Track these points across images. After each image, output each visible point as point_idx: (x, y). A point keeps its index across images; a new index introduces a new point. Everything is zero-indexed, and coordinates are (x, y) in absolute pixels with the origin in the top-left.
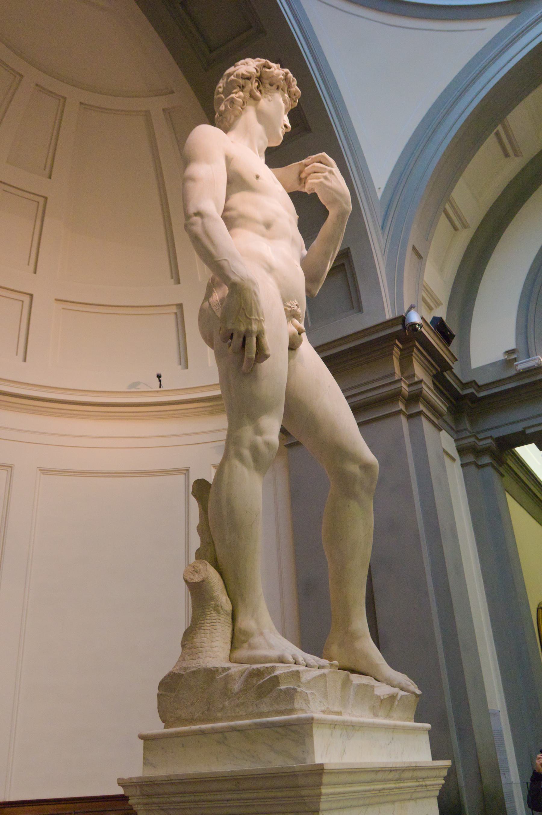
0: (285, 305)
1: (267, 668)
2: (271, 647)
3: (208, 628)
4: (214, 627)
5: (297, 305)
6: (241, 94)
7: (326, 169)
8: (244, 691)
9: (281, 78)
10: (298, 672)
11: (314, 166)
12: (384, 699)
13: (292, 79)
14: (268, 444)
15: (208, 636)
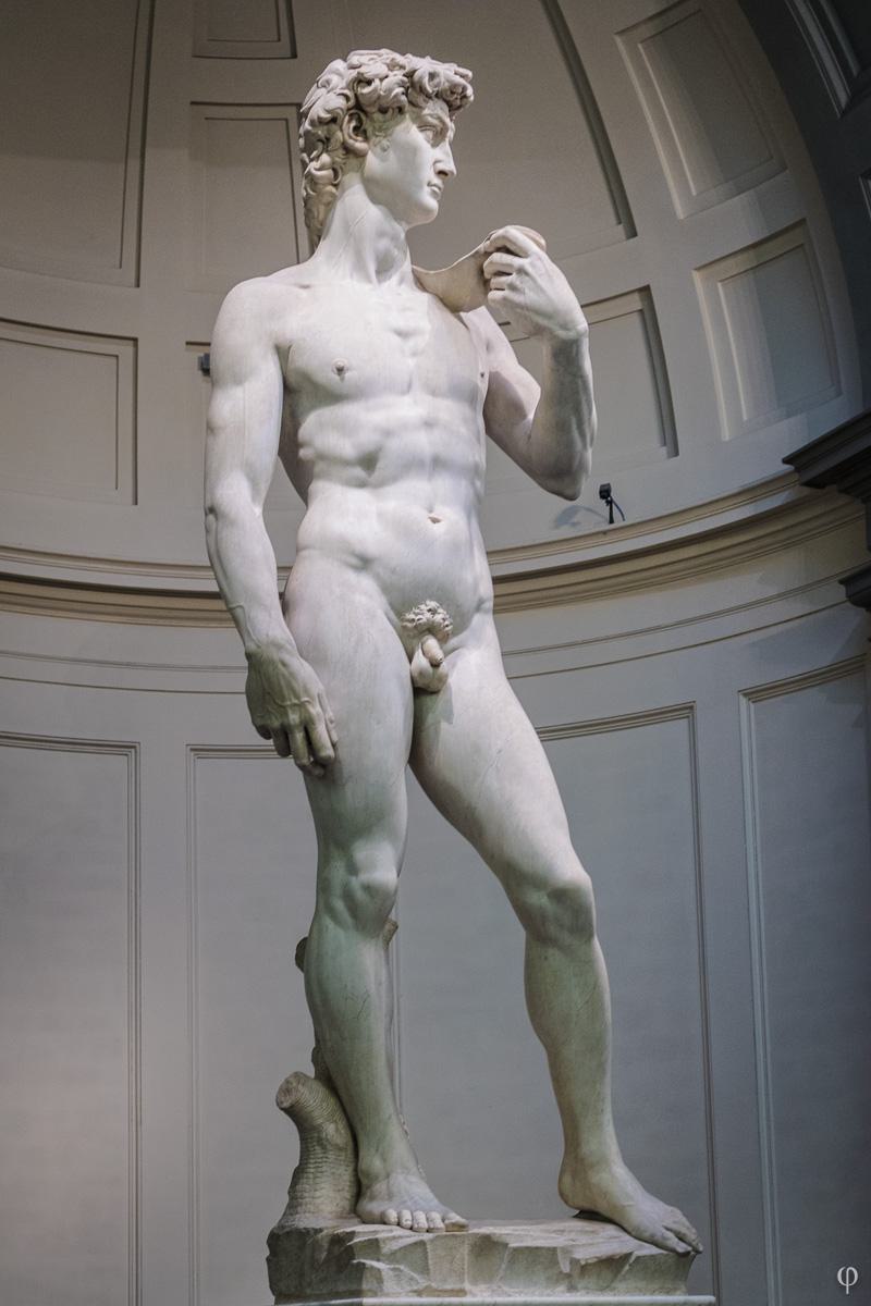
0: (402, 620)
1: (347, 1233)
2: (390, 1196)
3: (312, 1170)
4: (320, 1170)
5: (429, 610)
6: (325, 158)
7: (510, 266)
8: (327, 1261)
9: (396, 96)
10: (377, 1240)
11: (491, 263)
12: (586, 1265)
13: (426, 80)
14: (368, 888)
15: (311, 1182)
